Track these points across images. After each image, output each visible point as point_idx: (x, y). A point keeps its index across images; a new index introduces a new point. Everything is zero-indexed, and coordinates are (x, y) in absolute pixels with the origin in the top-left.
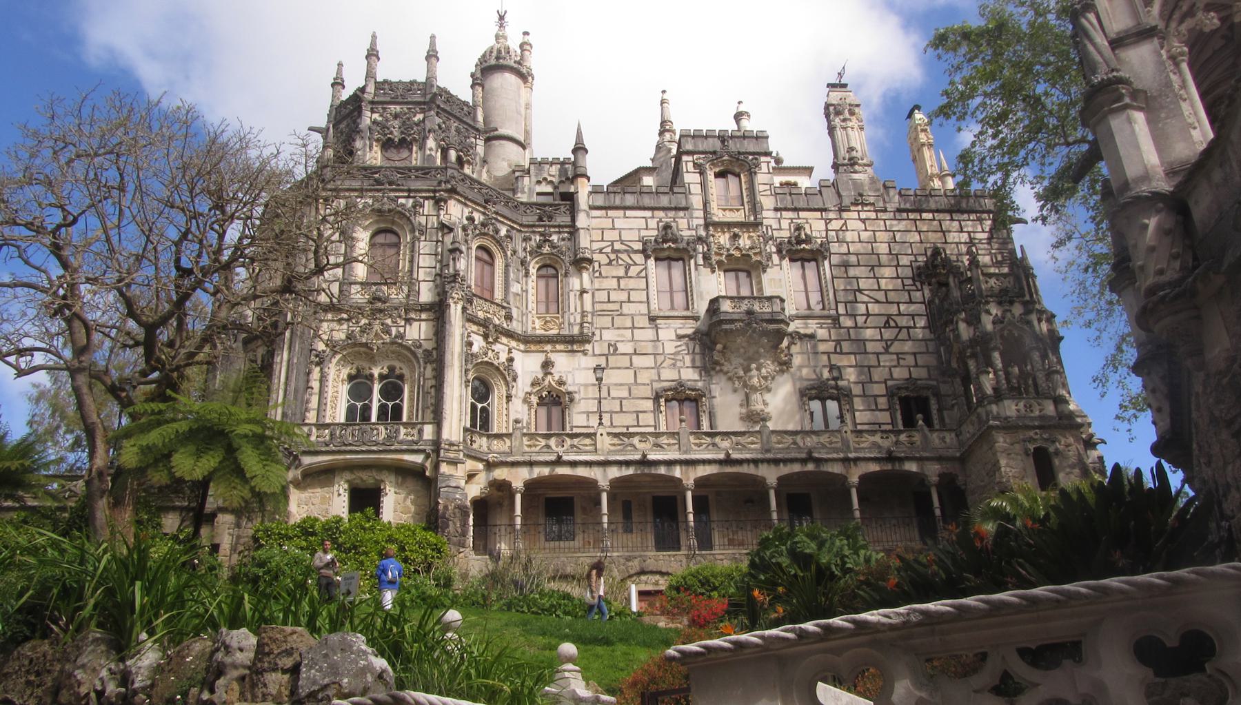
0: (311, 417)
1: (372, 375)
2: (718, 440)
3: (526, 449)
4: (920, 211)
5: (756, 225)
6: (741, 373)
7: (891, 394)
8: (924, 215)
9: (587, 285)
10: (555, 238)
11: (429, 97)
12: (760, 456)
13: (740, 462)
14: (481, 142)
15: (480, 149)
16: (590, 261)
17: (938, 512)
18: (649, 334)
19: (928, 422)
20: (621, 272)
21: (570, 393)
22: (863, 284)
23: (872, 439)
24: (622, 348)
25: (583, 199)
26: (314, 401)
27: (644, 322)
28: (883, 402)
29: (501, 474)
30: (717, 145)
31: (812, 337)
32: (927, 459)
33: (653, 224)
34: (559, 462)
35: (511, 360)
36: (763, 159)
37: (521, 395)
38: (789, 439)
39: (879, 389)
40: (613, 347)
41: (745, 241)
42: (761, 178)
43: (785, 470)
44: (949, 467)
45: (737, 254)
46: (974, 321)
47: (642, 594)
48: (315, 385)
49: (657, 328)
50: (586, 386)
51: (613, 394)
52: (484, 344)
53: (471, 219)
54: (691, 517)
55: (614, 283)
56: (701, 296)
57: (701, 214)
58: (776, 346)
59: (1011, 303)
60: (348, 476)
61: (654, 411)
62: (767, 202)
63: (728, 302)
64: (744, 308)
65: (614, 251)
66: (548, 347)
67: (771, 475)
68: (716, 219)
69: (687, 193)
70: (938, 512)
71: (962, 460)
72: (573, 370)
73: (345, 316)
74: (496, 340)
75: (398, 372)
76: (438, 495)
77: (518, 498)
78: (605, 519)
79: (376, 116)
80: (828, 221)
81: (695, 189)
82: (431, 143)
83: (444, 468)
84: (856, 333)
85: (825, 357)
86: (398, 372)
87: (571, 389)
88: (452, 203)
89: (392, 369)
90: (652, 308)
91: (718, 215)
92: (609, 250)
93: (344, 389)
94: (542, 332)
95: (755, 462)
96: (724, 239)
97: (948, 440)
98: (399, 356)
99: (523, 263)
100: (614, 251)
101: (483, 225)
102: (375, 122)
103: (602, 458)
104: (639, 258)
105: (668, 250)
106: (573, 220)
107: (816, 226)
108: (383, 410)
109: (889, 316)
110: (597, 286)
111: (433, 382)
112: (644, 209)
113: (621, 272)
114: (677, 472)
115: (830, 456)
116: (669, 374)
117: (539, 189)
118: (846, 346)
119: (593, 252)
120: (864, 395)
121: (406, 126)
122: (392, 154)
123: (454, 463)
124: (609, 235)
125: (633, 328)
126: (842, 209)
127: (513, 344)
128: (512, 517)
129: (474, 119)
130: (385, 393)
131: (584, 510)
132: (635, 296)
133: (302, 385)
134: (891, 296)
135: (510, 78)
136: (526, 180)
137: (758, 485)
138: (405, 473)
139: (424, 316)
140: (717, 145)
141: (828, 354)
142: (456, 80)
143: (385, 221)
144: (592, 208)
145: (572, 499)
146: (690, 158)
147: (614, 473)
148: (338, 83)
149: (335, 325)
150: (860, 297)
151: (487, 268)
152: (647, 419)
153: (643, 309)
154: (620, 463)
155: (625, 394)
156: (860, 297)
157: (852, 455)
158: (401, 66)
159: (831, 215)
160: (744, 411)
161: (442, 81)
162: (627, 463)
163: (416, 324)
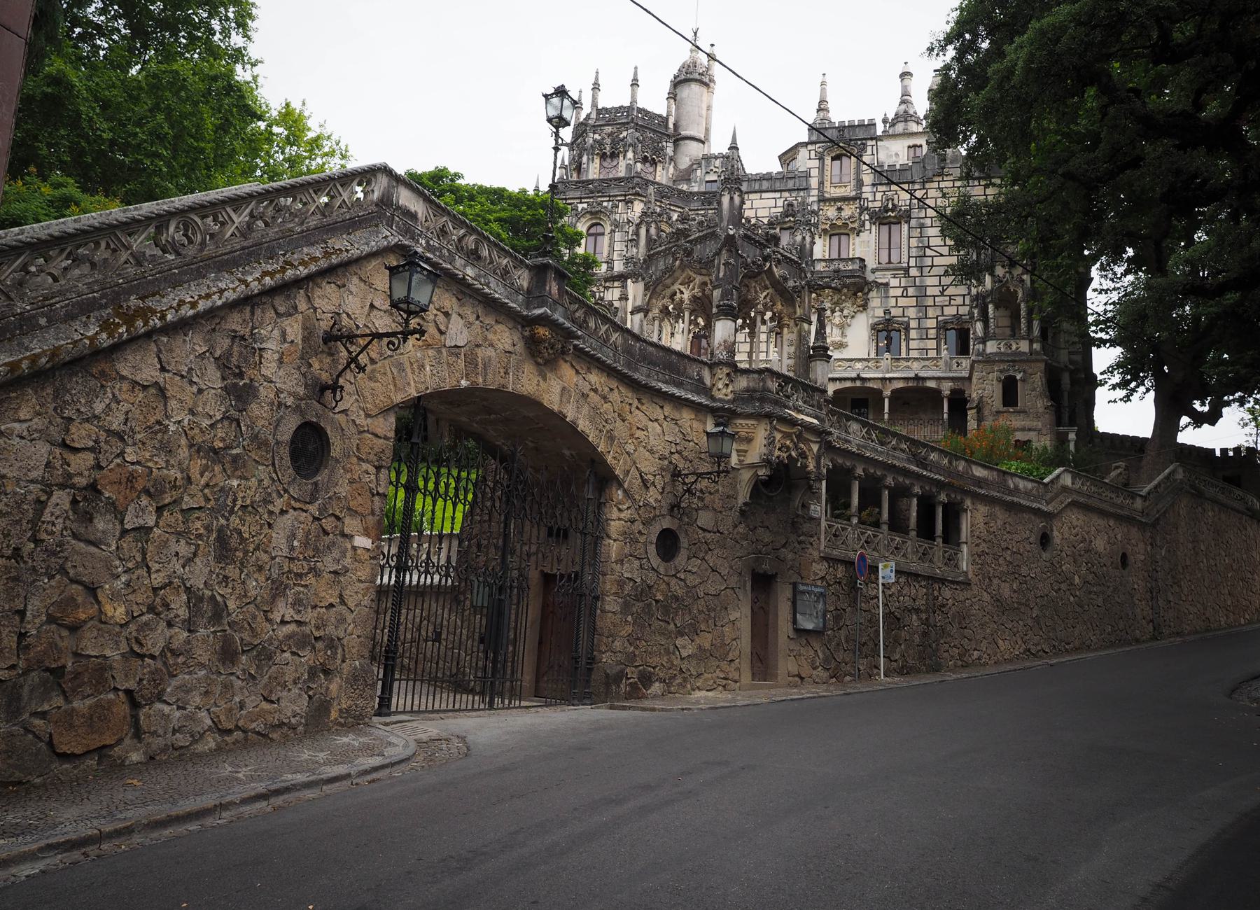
5: (857, 198)
7: (943, 327)
14: (670, 145)
22: (933, 242)
28: (932, 333)
31: (887, 285)
33: (780, 203)
36: (869, 143)
39: (931, 323)
41: (848, 211)
43: (838, 386)
44: (959, 385)
45: (839, 223)
57: (815, 192)
58: (855, 294)
63: (823, 264)
64: (832, 268)
68: (827, 195)
69: (807, 175)
81: (815, 172)
82: (630, 155)
88: (636, 203)
96: (831, 212)
102: (595, 141)
115: (872, 376)
117: (708, 178)
118: (911, 291)
121: (615, 143)
129: (667, 127)
135: (695, 87)
139: (616, 284)
142: (655, 100)
150: (928, 252)
157: (887, 376)
158: (615, 97)
161: (640, 105)
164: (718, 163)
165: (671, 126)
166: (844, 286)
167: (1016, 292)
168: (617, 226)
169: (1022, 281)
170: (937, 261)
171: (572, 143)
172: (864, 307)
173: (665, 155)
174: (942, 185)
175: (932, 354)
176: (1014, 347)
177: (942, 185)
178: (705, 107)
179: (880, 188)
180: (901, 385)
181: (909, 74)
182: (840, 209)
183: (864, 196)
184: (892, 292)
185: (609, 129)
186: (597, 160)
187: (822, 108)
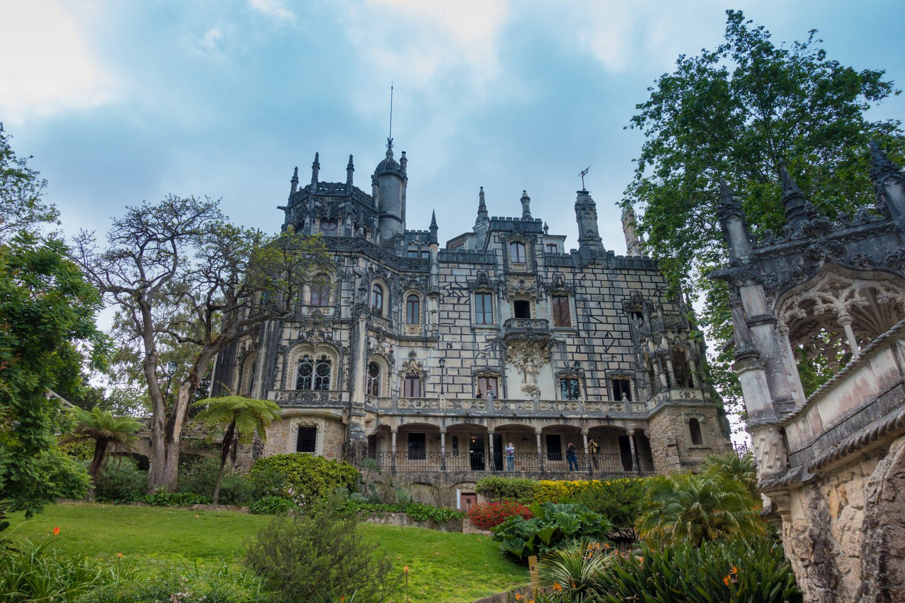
0: (278, 385)
1: (311, 361)
2: (507, 405)
3: (400, 407)
4: (628, 270)
5: (534, 274)
6: (522, 362)
8: (631, 272)
9: (437, 309)
10: (418, 279)
11: (346, 192)
12: (532, 415)
13: (521, 418)
14: (376, 220)
15: (376, 224)
16: (438, 294)
17: (633, 451)
18: (470, 338)
19: (629, 397)
20: (455, 301)
21: (425, 372)
22: (594, 312)
23: (596, 407)
24: (455, 346)
25: (434, 256)
26: (279, 377)
27: (467, 331)
28: (603, 382)
29: (385, 421)
30: (512, 226)
31: (564, 343)
32: (628, 420)
33: (474, 273)
34: (418, 415)
35: (392, 352)
36: (539, 235)
37: (396, 372)
38: (550, 405)
39: (601, 375)
40: (450, 345)
41: (528, 284)
42: (537, 247)
45: (523, 292)
46: (656, 342)
47: (463, 494)
48: (280, 366)
49: (475, 335)
50: (433, 367)
51: (449, 373)
52: (376, 343)
53: (371, 269)
54: (492, 450)
55: (451, 307)
56: (500, 316)
57: (501, 267)
58: (542, 348)
59: (679, 332)
60: (298, 421)
61: (472, 384)
62: (540, 262)
65: (451, 288)
66: (413, 344)
67: (538, 426)
70: (633, 451)
71: (648, 421)
72: (428, 358)
73: (298, 325)
74: (384, 340)
75: (327, 359)
76: (349, 436)
77: (394, 436)
78: (443, 450)
79: (317, 203)
80: (575, 274)
81: (500, 253)
82: (349, 222)
83: (354, 419)
84: (589, 342)
85: (570, 355)
86: (327, 359)
87: (425, 369)
88: (361, 259)
89: (324, 357)
90: (473, 322)
91: (513, 269)
92: (449, 287)
93: (296, 369)
94: (408, 335)
95: (529, 418)
96: (515, 283)
97: (640, 409)
98: (328, 349)
99: (400, 293)
100: (451, 288)
101: (377, 272)
102: (316, 207)
103: (442, 414)
104: (465, 293)
105: (482, 288)
106: (429, 269)
107: (568, 277)
108: (318, 380)
109: (608, 332)
110: (441, 309)
111: (346, 367)
112: (470, 264)
113: (455, 301)
114: (485, 424)
116: (480, 362)
117: (410, 248)
118: (583, 349)
119: (439, 288)
120: (592, 378)
121: (335, 211)
122: (325, 226)
123: (359, 416)
124: (449, 279)
125: (461, 334)
126: (582, 267)
127: (393, 342)
128: (390, 446)
129: (373, 206)
130: (319, 370)
131: (431, 441)
132: (463, 315)
133: (273, 365)
134: (610, 320)
135: (394, 179)
136: (402, 243)
137: (531, 431)
138: (329, 419)
139: (344, 326)
140: (512, 226)
141: (572, 353)
143: (322, 269)
144: (440, 262)
145: (424, 435)
146: (496, 234)
147: (449, 422)
148: (295, 181)
149: (293, 330)
150: (592, 320)
151: (379, 297)
152: (469, 388)
153: (467, 323)
154: (453, 417)
155: (456, 373)
156: (592, 320)
158: (333, 173)
159: (577, 271)
160: (524, 385)
161: (355, 184)
162: (457, 417)
163: (339, 331)
164: (418, 237)
165: (377, 205)
166: (537, 341)
167: (684, 352)
168: (344, 277)
169: (689, 344)
170: (599, 327)
171: (290, 208)
172: (549, 359)
173: (374, 227)
174: (595, 271)
175: (605, 399)
176: (692, 396)
177: (595, 271)
178: (401, 195)
179: (550, 269)
180: (595, 424)
181: (529, 199)
182: (522, 282)
183: (539, 273)
184: (569, 349)
185: (329, 199)
186: (318, 223)
187: (482, 209)
